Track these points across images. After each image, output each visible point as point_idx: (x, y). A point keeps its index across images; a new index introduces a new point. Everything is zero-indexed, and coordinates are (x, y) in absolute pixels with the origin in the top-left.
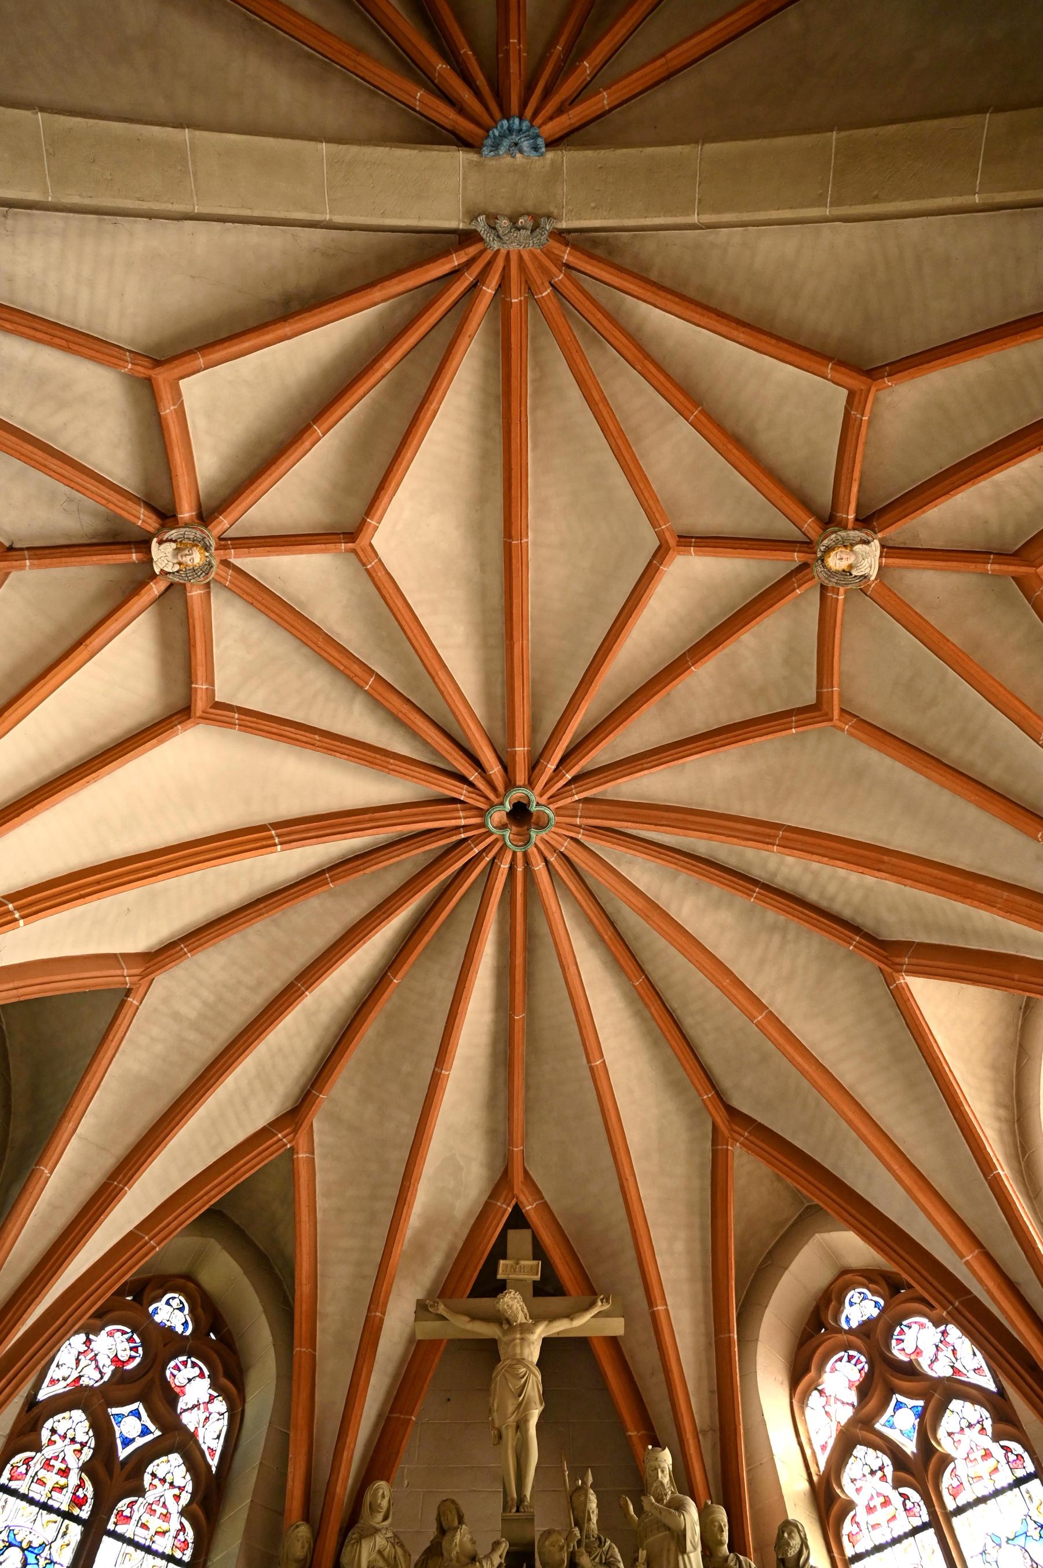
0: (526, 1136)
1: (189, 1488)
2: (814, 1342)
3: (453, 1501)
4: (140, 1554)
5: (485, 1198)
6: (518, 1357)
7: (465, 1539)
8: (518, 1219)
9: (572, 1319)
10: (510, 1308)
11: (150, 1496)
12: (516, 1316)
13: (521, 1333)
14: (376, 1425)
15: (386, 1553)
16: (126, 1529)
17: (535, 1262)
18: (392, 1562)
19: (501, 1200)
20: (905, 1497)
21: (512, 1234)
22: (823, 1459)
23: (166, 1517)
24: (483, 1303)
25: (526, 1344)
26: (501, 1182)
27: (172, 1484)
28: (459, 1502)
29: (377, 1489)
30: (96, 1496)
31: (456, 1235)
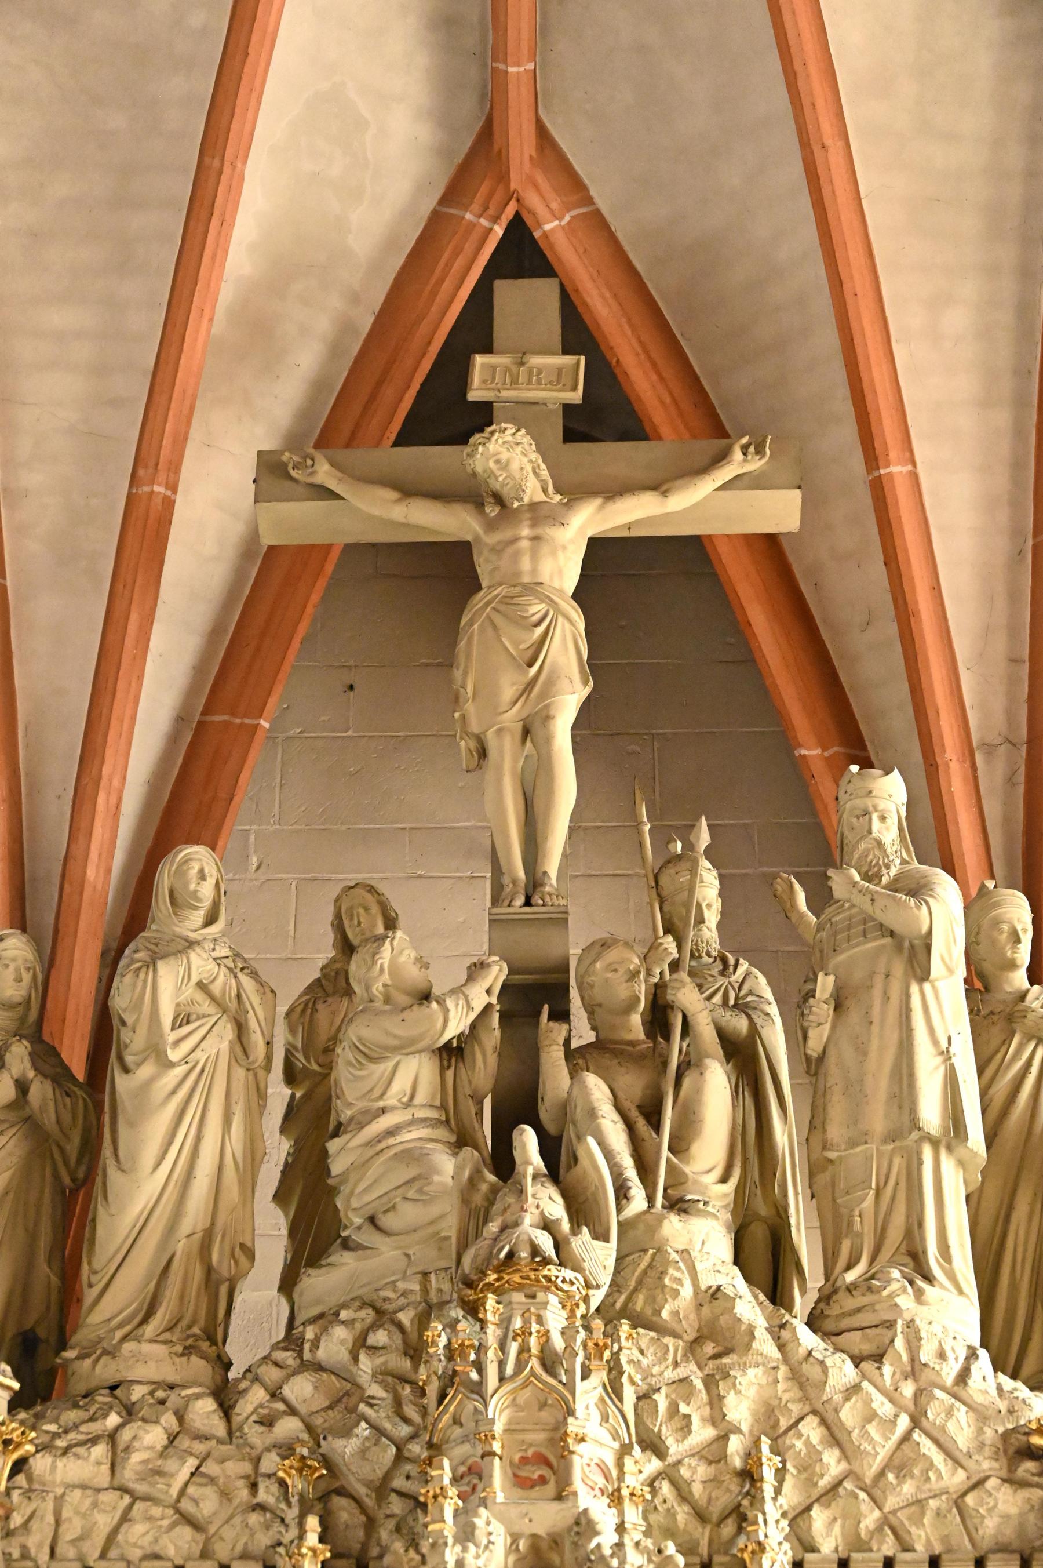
0: (543, 31)
3: (371, 889)
5: (429, 204)
6: (526, 579)
7: (403, 959)
8: (521, 253)
9: (665, 494)
10: (505, 466)
12: (520, 488)
13: (533, 526)
14: (173, 739)
15: (216, 988)
17: (569, 360)
18: (233, 1005)
19: (476, 207)
21: (505, 291)
24: (436, 459)
25: (545, 549)
26: (477, 161)
28: (381, 887)
29: (187, 861)
31: (355, 299)
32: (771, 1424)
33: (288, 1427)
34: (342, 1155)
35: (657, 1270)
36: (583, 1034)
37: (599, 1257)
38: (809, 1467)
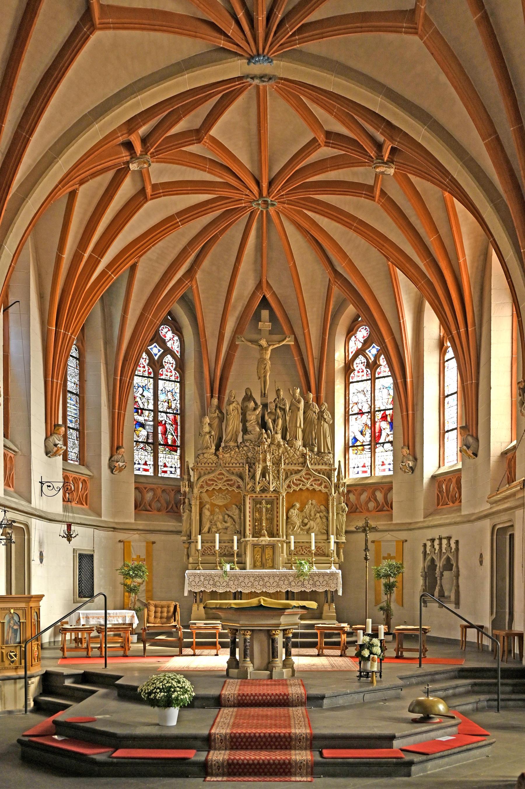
1: (174, 363)
2: (356, 322)
4: (168, 382)
11: (166, 367)
16: (163, 377)
20: (367, 371)
22: (351, 356)
23: (171, 372)
27: (170, 363)
30: (153, 371)
32: (283, 453)
33: (244, 452)
34: (248, 424)
35: (274, 439)
36: (269, 411)
37: (269, 440)
38: (286, 456)
